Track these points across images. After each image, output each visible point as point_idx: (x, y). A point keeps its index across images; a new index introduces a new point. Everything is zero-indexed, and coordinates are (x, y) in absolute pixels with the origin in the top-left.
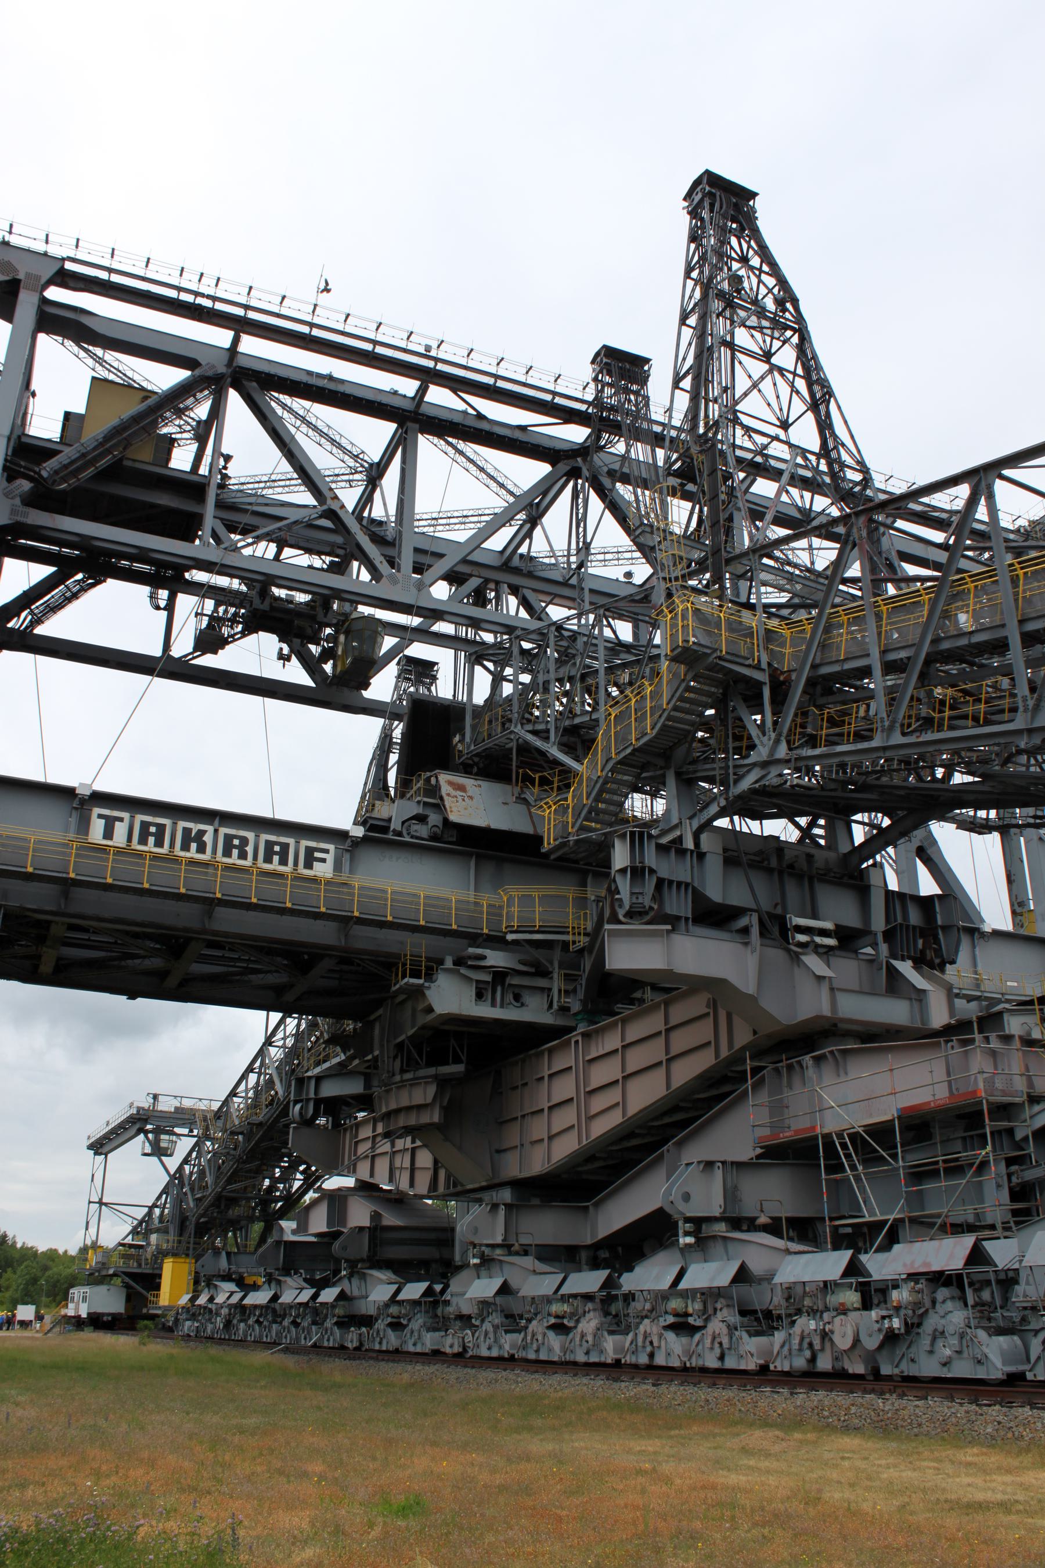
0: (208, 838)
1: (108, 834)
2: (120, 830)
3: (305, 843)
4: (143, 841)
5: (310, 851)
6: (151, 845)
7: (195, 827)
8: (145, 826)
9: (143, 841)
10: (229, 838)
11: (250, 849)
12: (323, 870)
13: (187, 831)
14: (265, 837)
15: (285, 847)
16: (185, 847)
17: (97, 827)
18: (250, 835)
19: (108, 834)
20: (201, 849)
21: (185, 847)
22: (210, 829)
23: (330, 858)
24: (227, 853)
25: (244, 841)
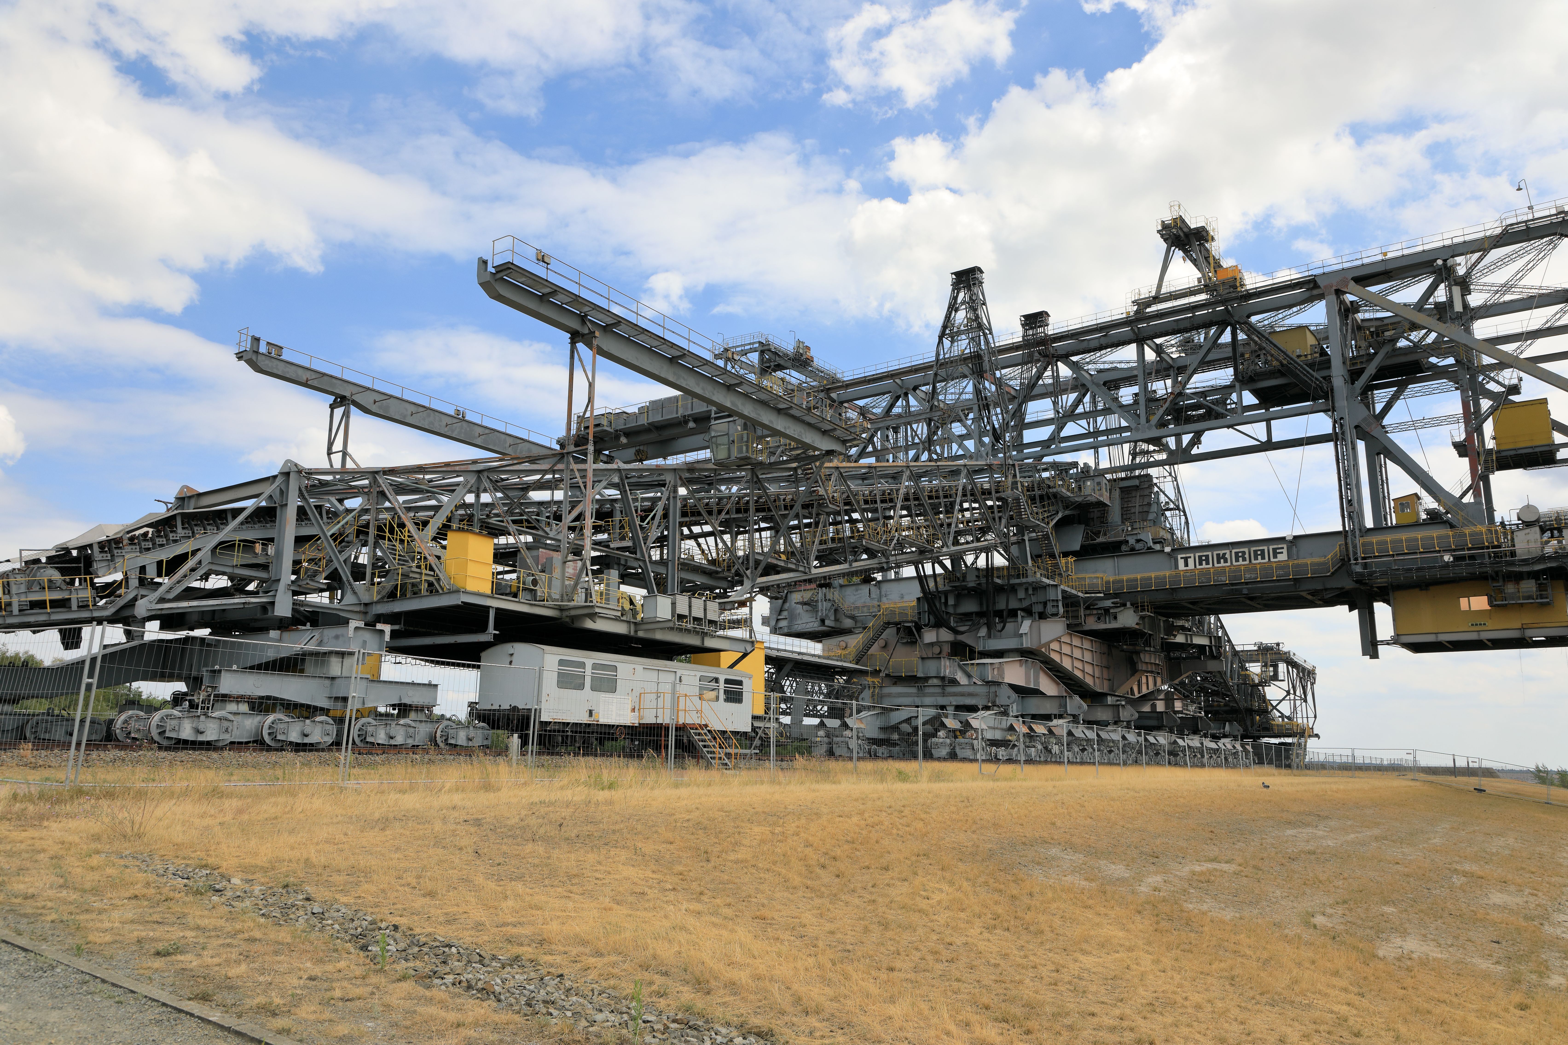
0: (1227, 556)
1: (1186, 565)
2: (1191, 562)
3: (1271, 547)
4: (1201, 564)
5: (1274, 550)
6: (1204, 566)
7: (1221, 552)
8: (1200, 557)
9: (1201, 564)
10: (1237, 553)
11: (1247, 556)
12: (1283, 557)
13: (1218, 555)
14: (1253, 549)
15: (1263, 551)
16: (1219, 562)
17: (1181, 563)
18: (1246, 550)
19: (1186, 565)
20: (1226, 561)
21: (1219, 562)
22: (1228, 552)
23: (1285, 551)
24: (1237, 560)
25: (1244, 553)
